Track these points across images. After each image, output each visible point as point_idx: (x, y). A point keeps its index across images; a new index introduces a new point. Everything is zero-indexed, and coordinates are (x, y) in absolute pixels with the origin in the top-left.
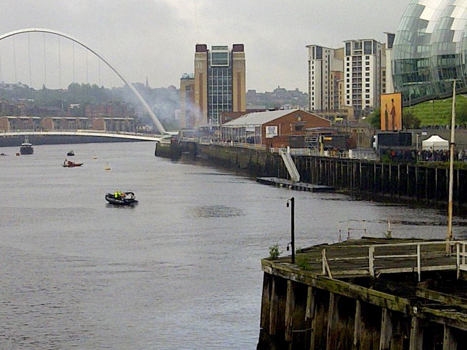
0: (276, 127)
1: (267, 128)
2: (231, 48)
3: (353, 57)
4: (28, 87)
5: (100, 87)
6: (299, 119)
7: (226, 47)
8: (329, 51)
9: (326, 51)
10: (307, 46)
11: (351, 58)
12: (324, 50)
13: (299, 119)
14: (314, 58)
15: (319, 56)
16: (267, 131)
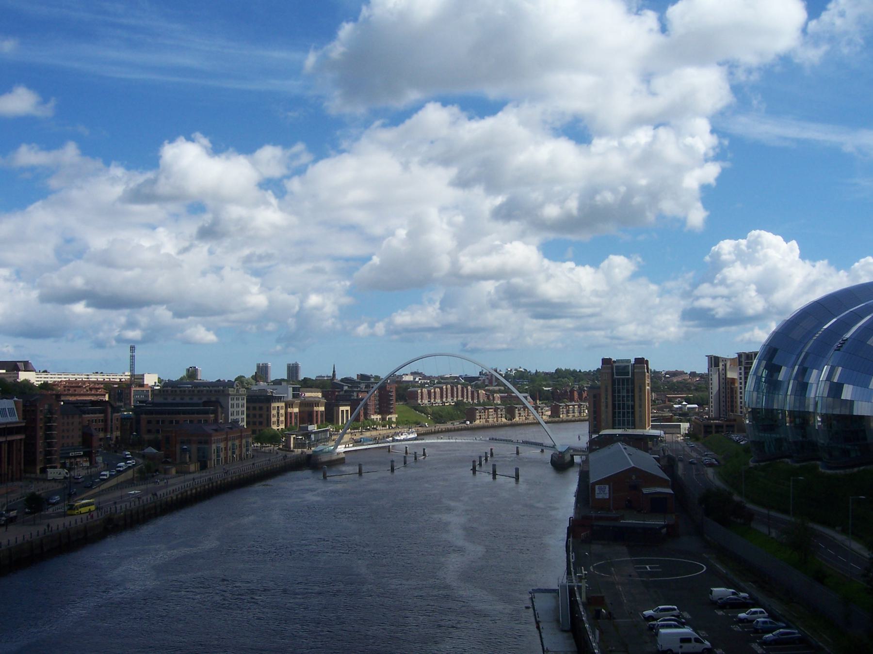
0: (607, 487)
1: (597, 487)
2: (633, 361)
3: (745, 367)
4: (527, 370)
5: (578, 371)
6: (634, 477)
7: (629, 361)
8: (725, 361)
9: (723, 361)
10: (706, 356)
11: (743, 368)
12: (720, 360)
13: (634, 477)
14: (712, 367)
15: (717, 365)
16: (597, 491)
